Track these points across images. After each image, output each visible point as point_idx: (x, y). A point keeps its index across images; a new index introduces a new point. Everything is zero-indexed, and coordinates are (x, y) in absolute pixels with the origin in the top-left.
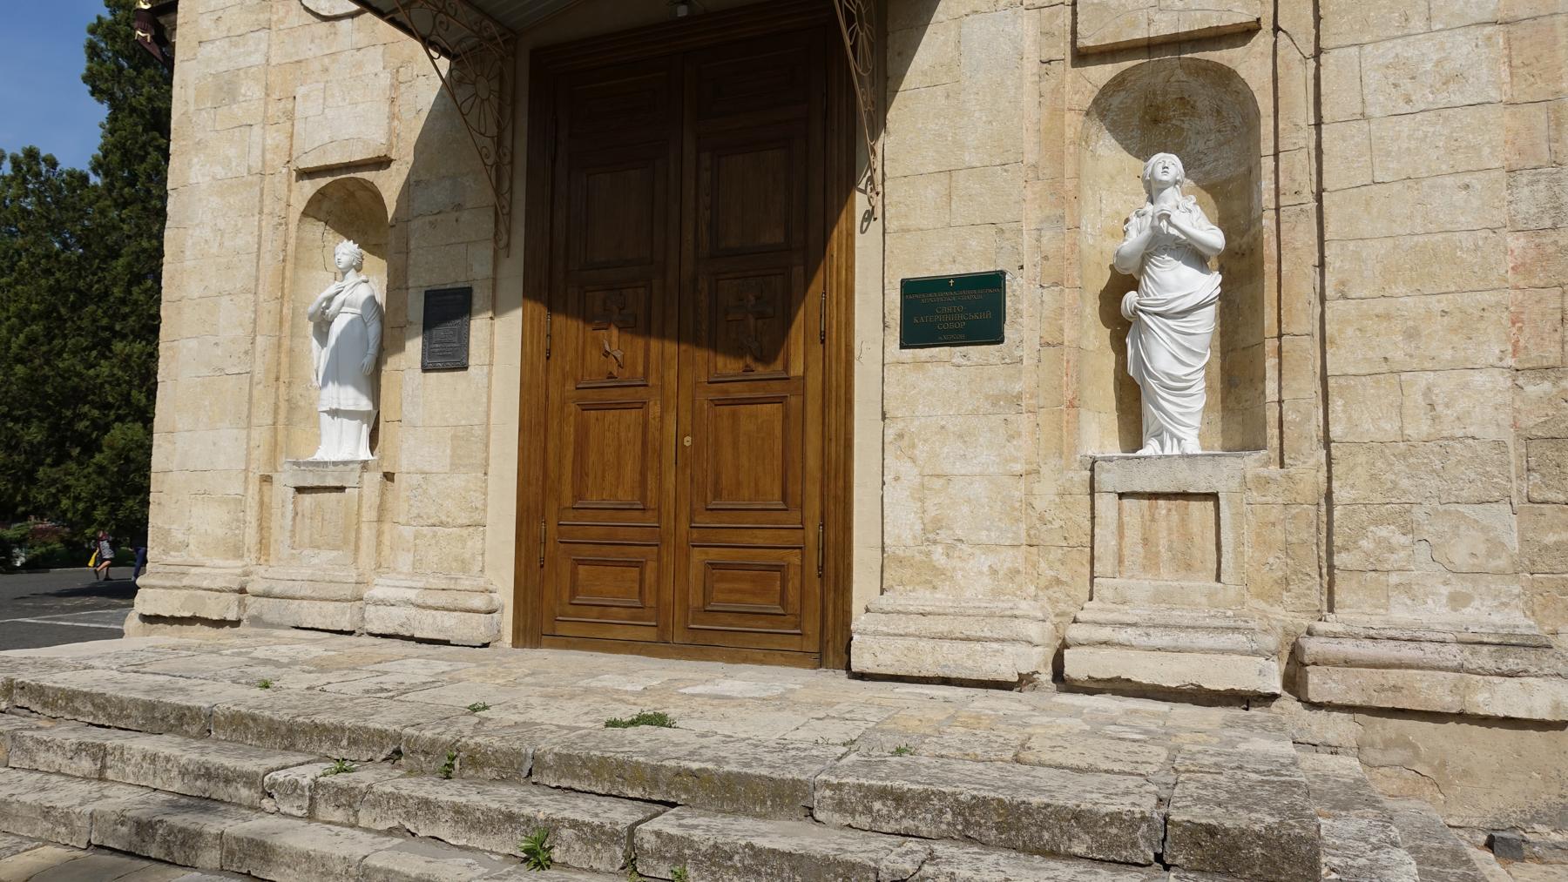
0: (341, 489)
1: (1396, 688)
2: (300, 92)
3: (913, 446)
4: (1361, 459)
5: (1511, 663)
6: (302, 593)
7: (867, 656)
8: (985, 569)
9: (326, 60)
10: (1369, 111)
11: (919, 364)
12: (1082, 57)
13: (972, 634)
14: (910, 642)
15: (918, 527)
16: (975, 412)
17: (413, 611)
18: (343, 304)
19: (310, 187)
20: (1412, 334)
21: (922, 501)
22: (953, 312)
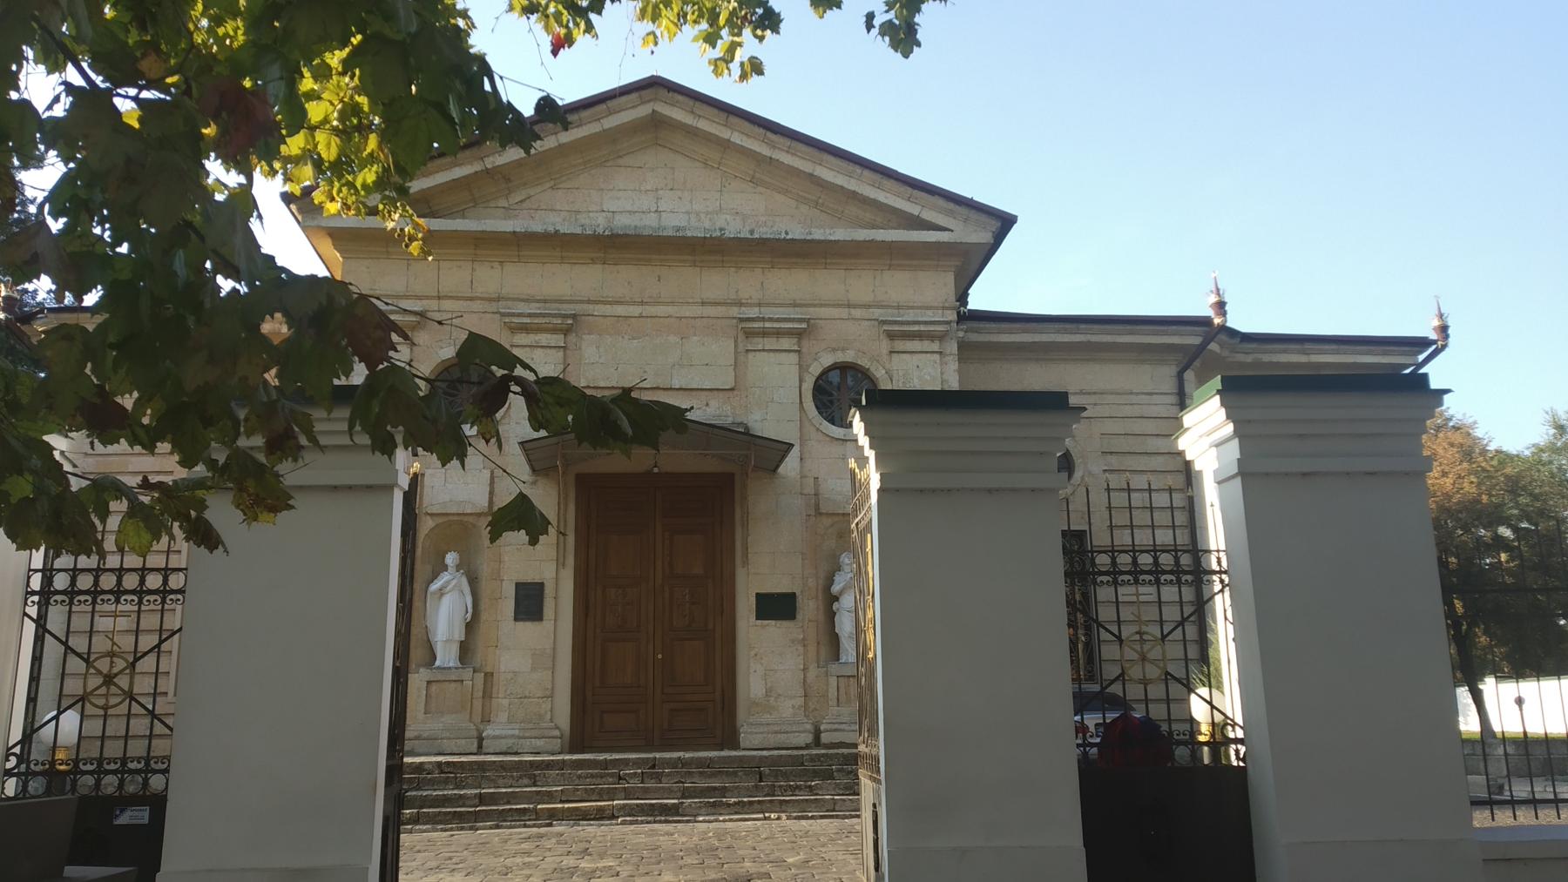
11: (763, 627)
22: (776, 607)
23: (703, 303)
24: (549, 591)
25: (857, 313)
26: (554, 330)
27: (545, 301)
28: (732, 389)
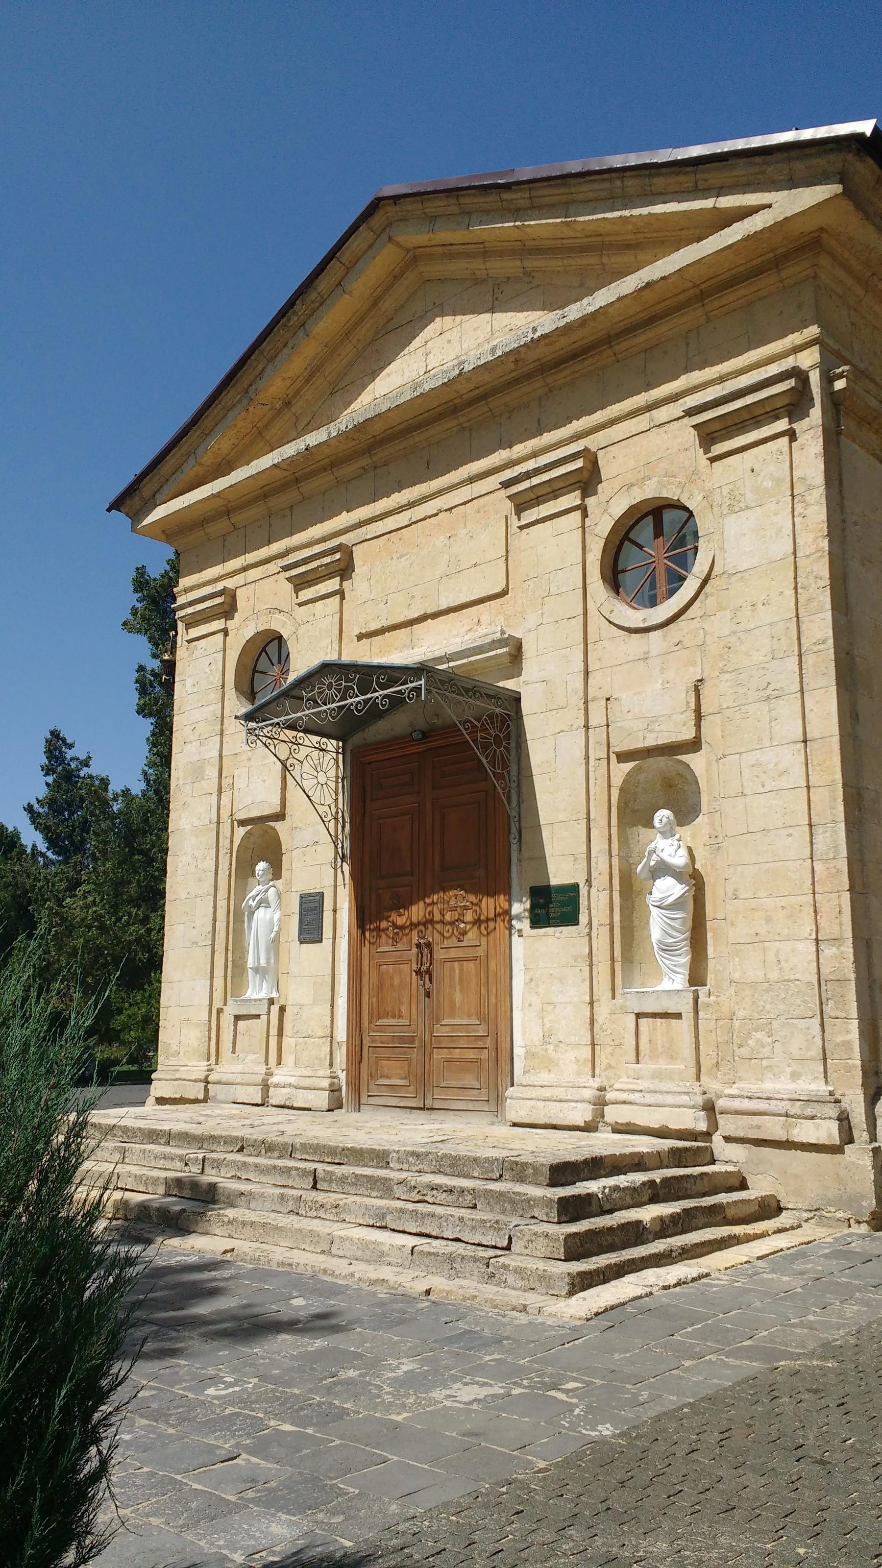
1: (758, 1127)
2: (237, 773)
3: (538, 986)
4: (748, 992)
5: (809, 1112)
6: (238, 1081)
7: (513, 1112)
8: (573, 1059)
10: (745, 792)
13: (562, 1097)
14: (532, 1103)
17: (293, 1090)
19: (240, 832)
20: (768, 920)
21: (543, 1018)
28: (504, 593)
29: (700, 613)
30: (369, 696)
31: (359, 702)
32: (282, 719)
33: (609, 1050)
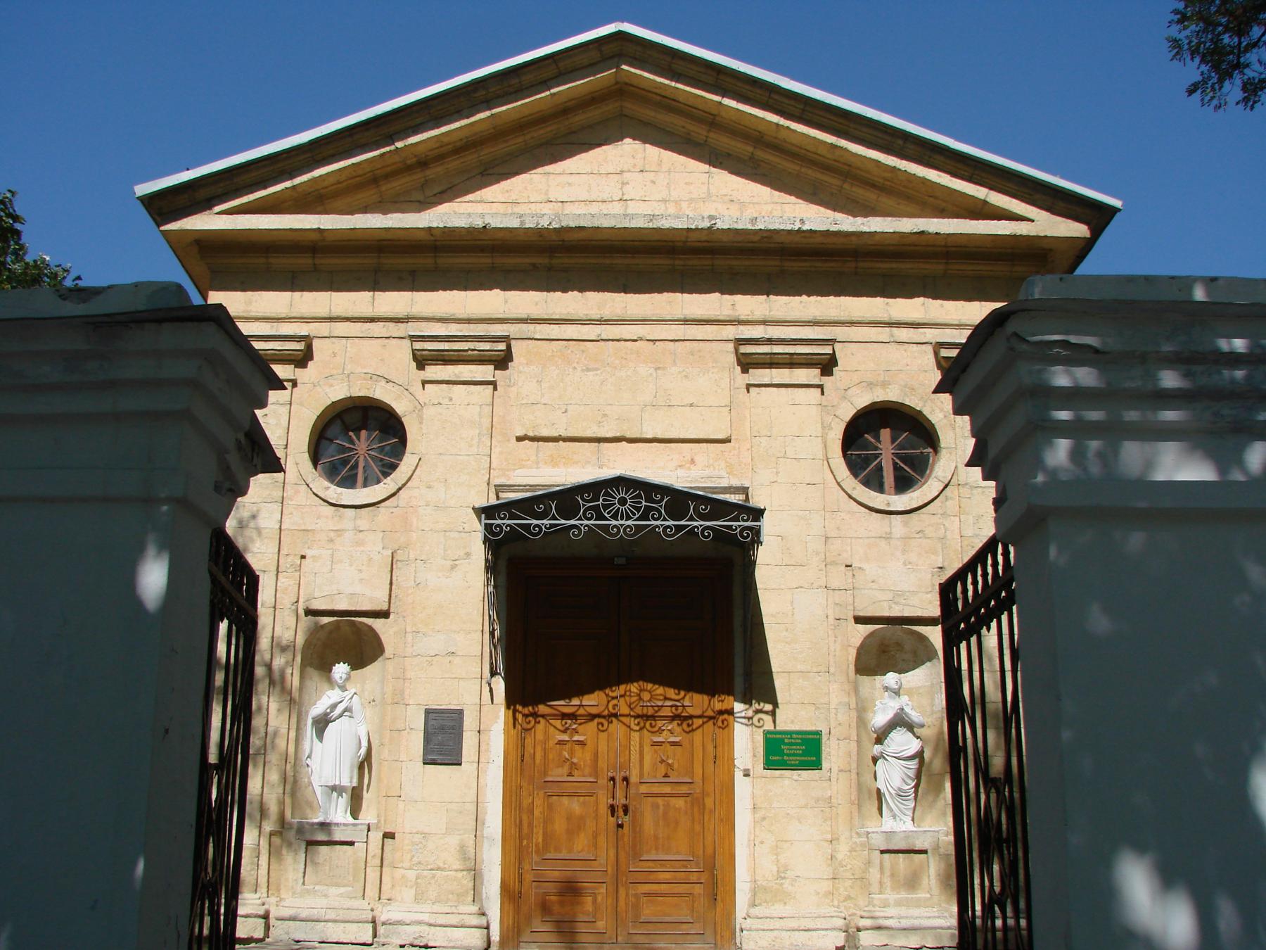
0: (352, 843)
6: (327, 917)
9: (332, 534)
12: (859, 620)
13: (811, 926)
14: (776, 933)
15: (775, 869)
16: (806, 806)
17: (426, 928)
18: (345, 711)
23: (686, 321)
24: (469, 723)
25: (903, 334)
26: (480, 360)
27: (469, 321)
28: (727, 441)
29: (940, 511)
30: (682, 523)
31: (668, 527)
32: (546, 522)
33: (848, 883)
